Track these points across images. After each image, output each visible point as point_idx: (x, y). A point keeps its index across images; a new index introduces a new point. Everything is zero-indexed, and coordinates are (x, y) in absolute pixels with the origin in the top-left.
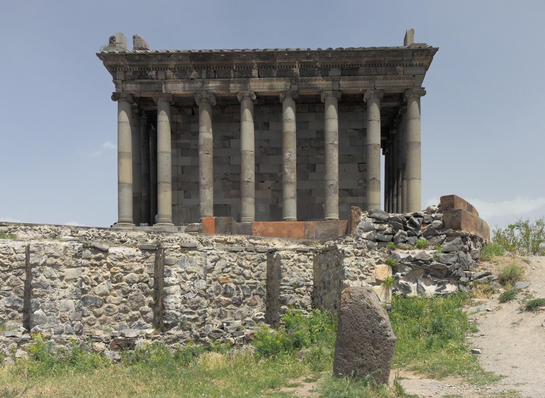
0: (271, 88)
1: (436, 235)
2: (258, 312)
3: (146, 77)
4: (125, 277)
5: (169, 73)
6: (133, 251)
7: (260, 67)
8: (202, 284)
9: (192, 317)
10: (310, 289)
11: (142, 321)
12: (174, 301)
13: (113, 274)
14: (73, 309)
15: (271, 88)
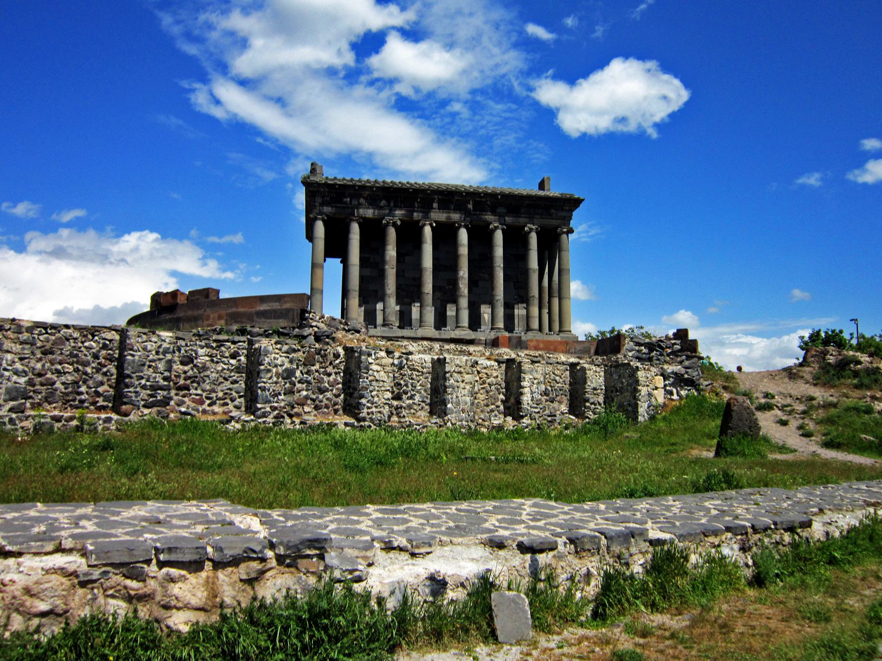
0: (448, 218)
1: (677, 356)
2: (564, 408)
3: (342, 202)
4: (488, 381)
5: (362, 200)
6: (493, 363)
7: (439, 202)
8: (543, 387)
9: (537, 410)
10: (603, 392)
11: (496, 412)
12: (526, 399)
13: (480, 378)
14: (469, 404)
15: (448, 218)
